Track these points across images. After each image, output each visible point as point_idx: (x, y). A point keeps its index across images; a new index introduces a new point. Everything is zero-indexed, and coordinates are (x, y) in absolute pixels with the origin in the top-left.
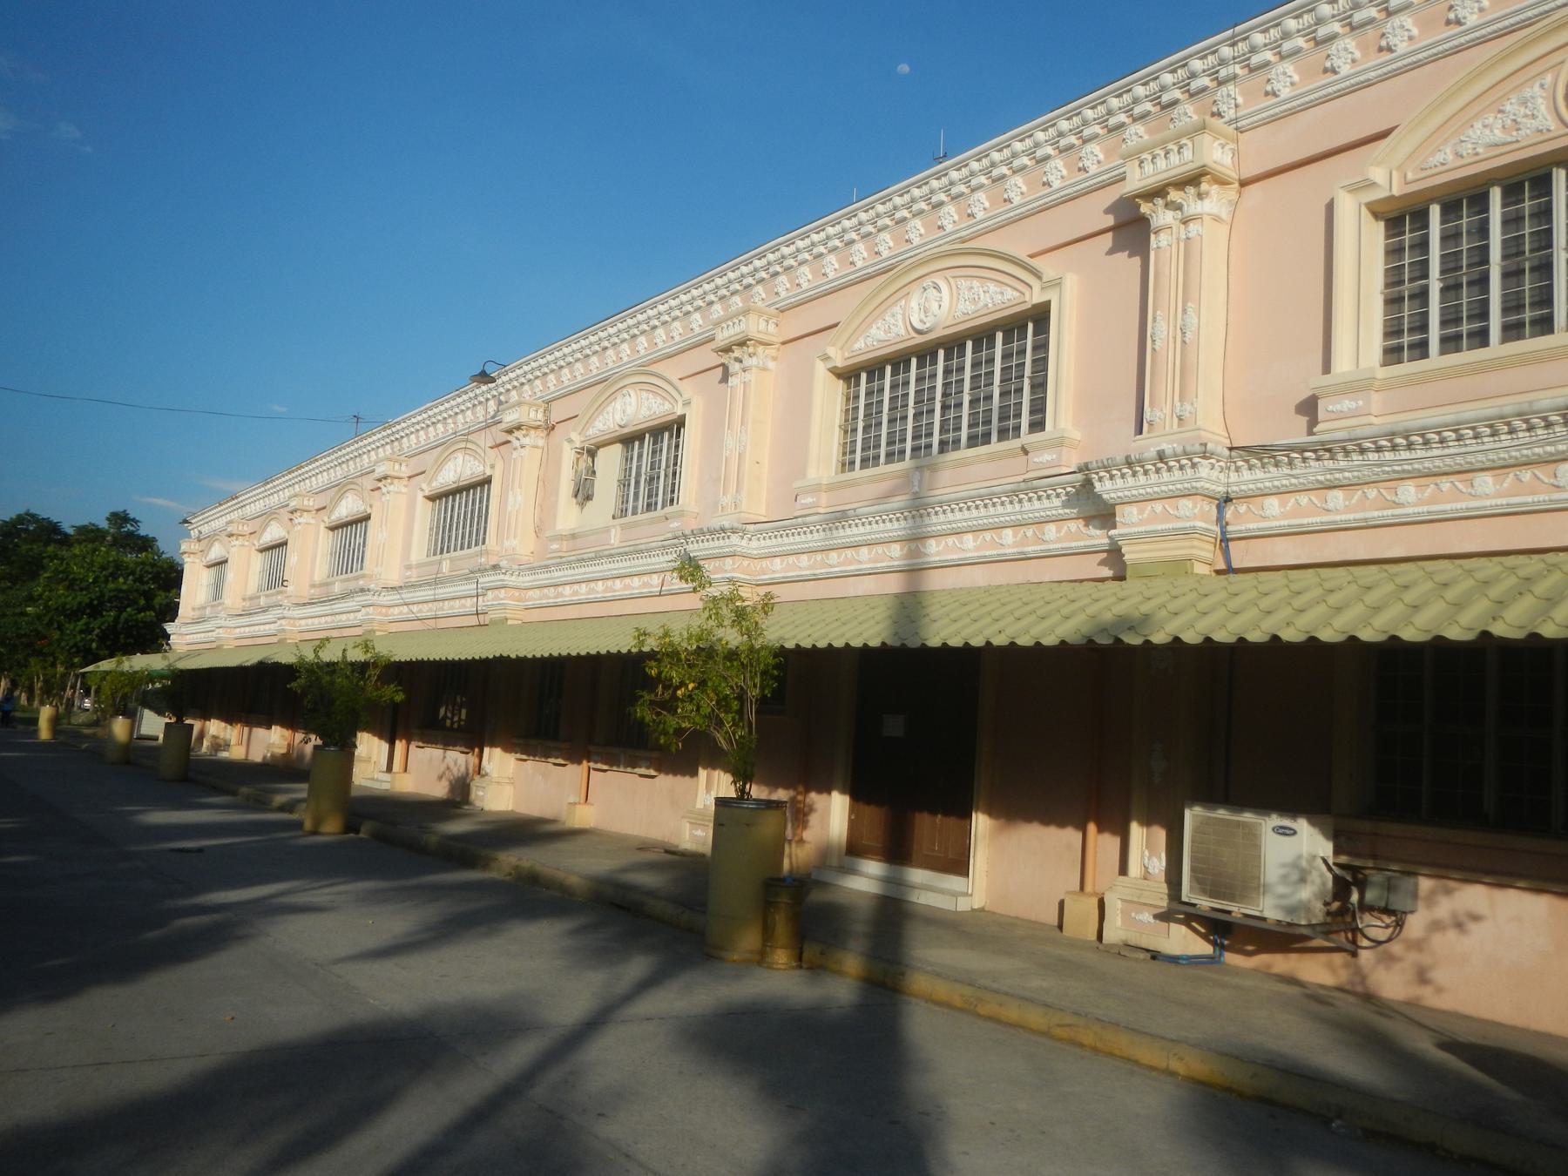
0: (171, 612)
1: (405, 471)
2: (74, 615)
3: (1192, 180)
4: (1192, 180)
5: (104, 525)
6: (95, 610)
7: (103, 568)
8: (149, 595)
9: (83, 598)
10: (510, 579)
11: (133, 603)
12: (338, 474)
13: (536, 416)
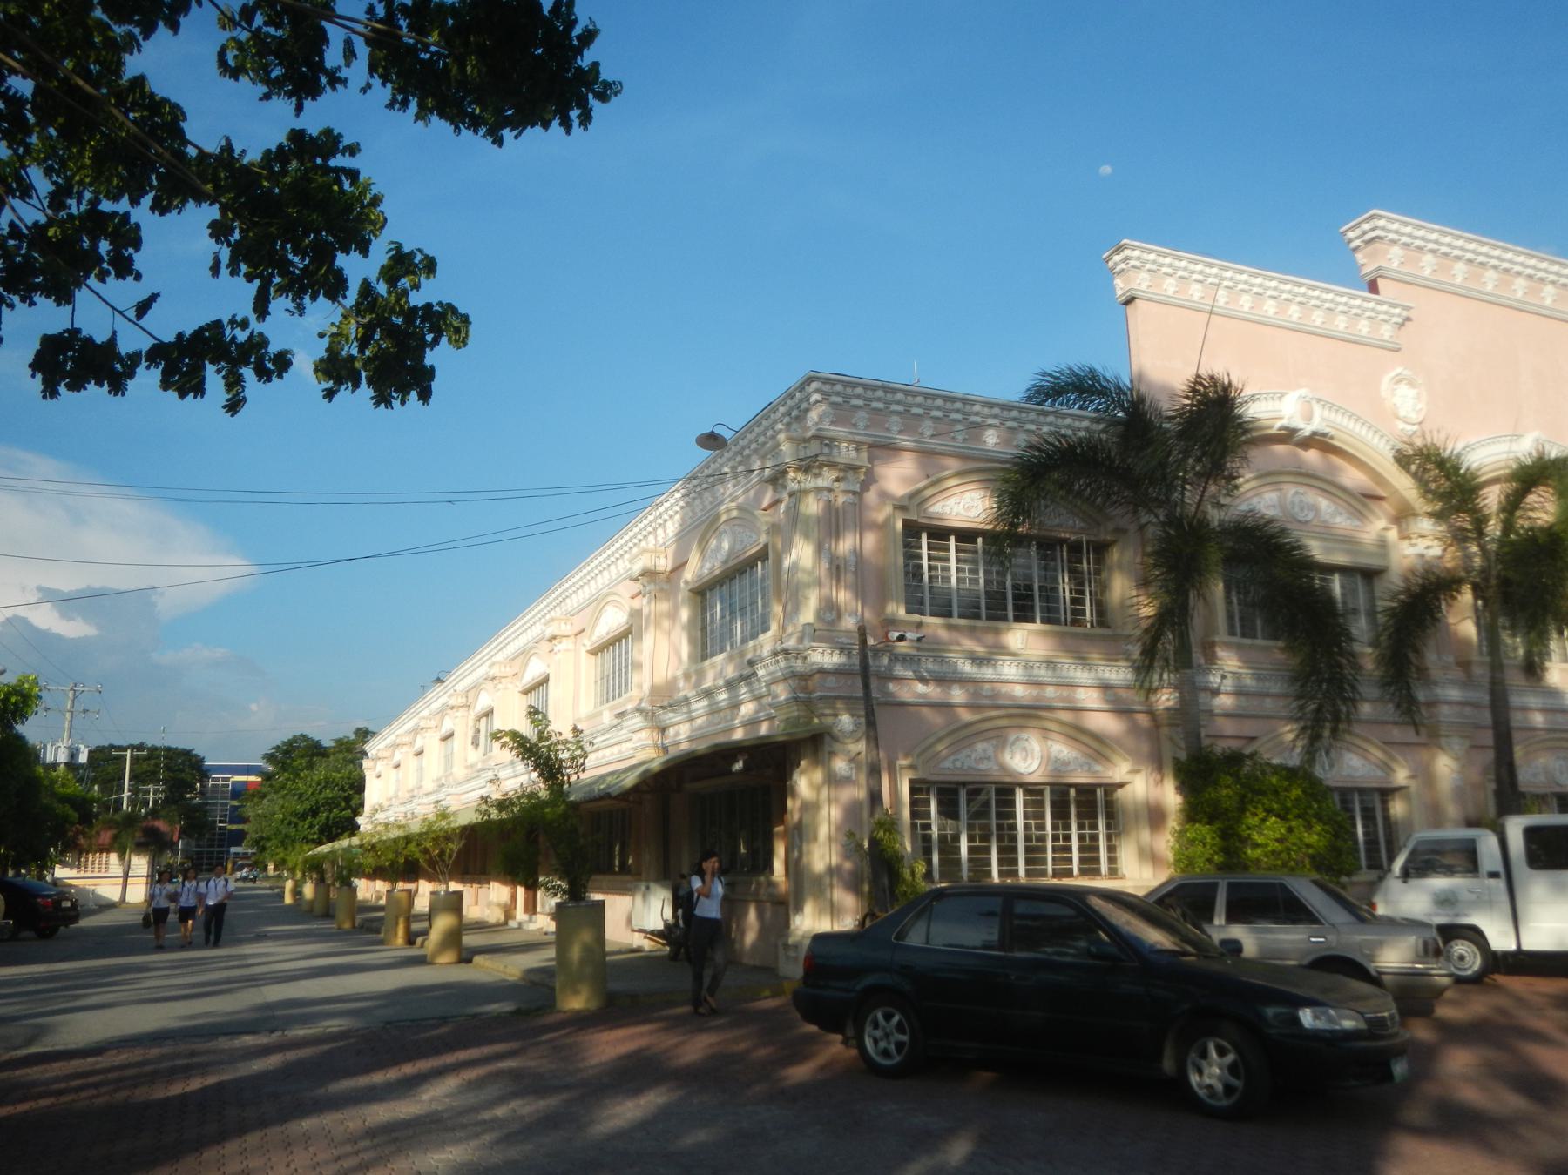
0: (358, 809)
1: (433, 723)
2: (303, 817)
3: (554, 637)
4: (554, 637)
5: (353, 737)
6: (314, 812)
7: (319, 783)
8: (348, 799)
9: (307, 805)
10: (450, 790)
11: (337, 805)
12: (410, 725)
13: (461, 700)
